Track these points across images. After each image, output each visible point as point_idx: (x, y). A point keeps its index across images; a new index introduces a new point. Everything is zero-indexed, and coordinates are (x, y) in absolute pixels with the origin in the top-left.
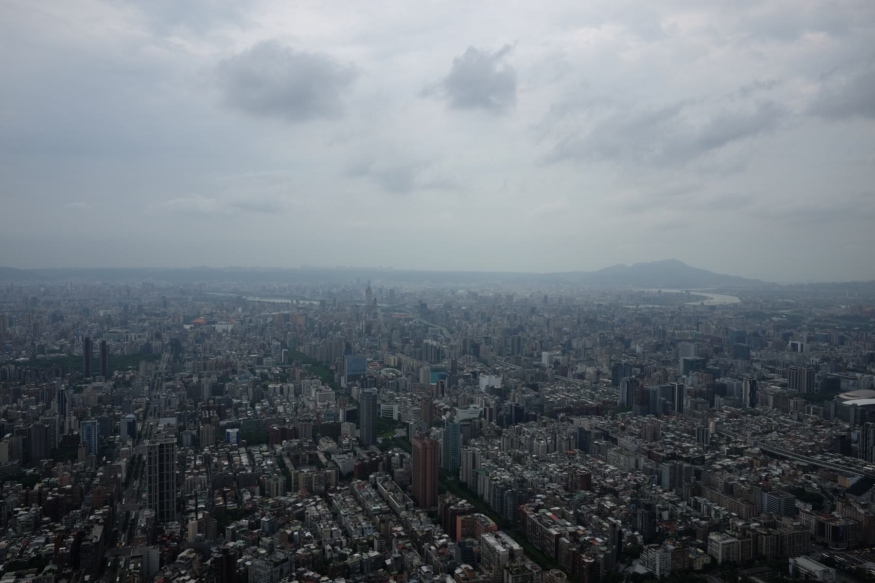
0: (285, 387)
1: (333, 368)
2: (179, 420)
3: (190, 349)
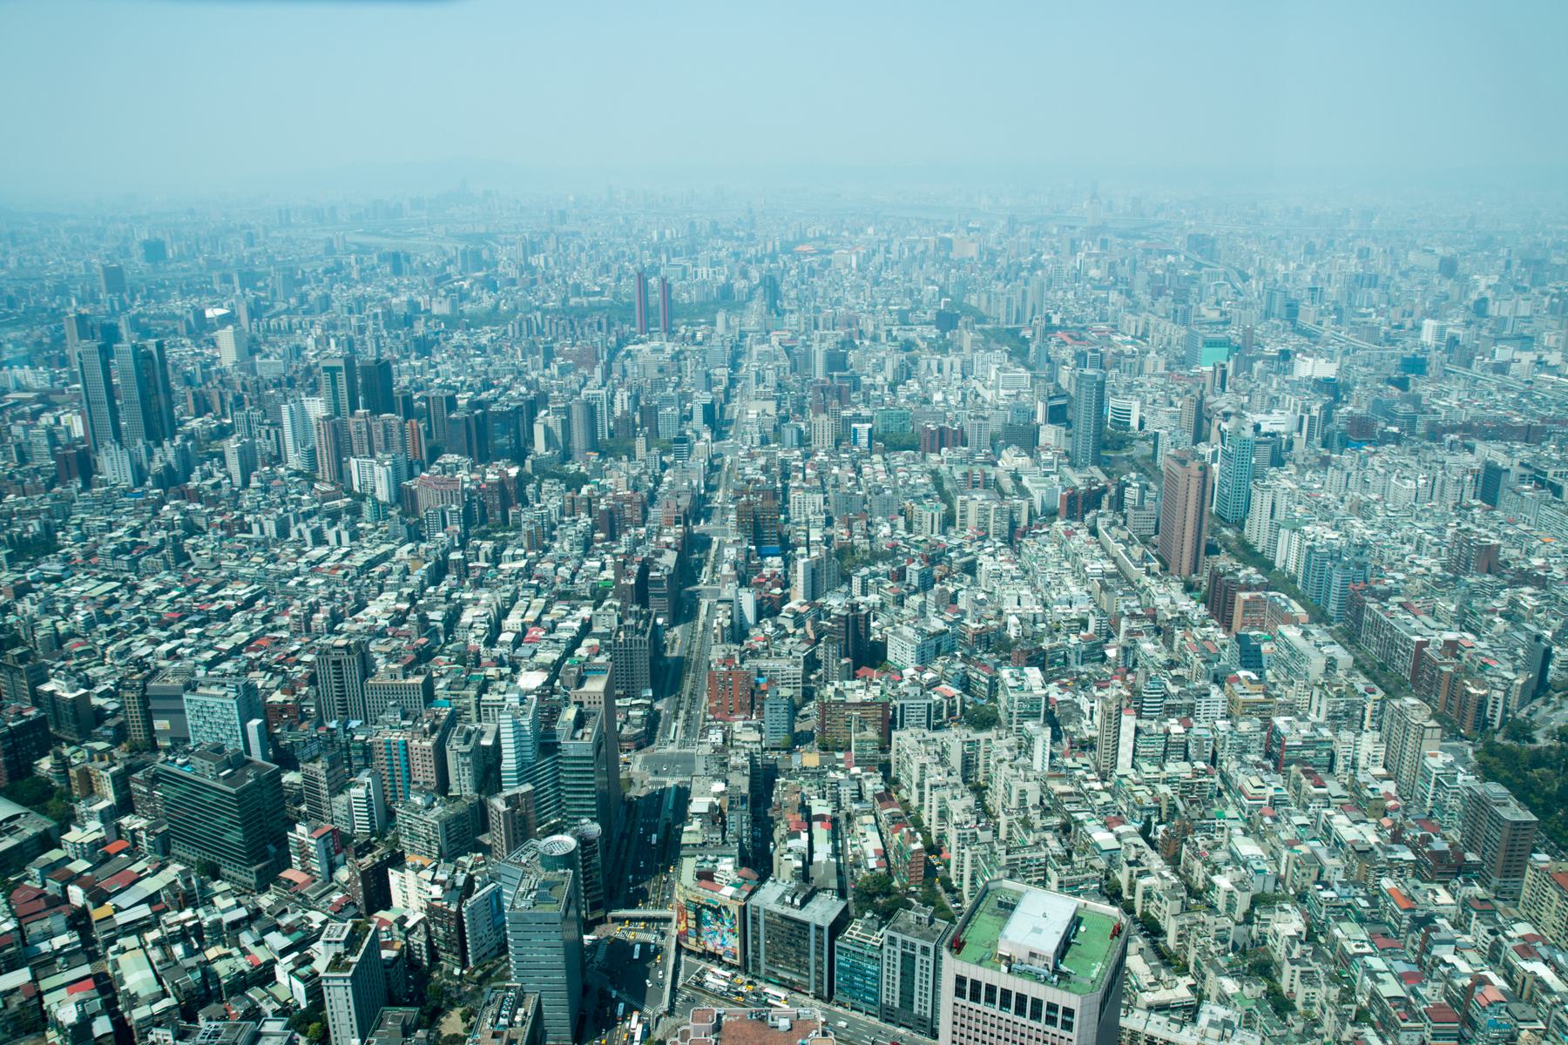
0: (947, 361)
1: (1028, 334)
2: (779, 407)
3: (792, 294)
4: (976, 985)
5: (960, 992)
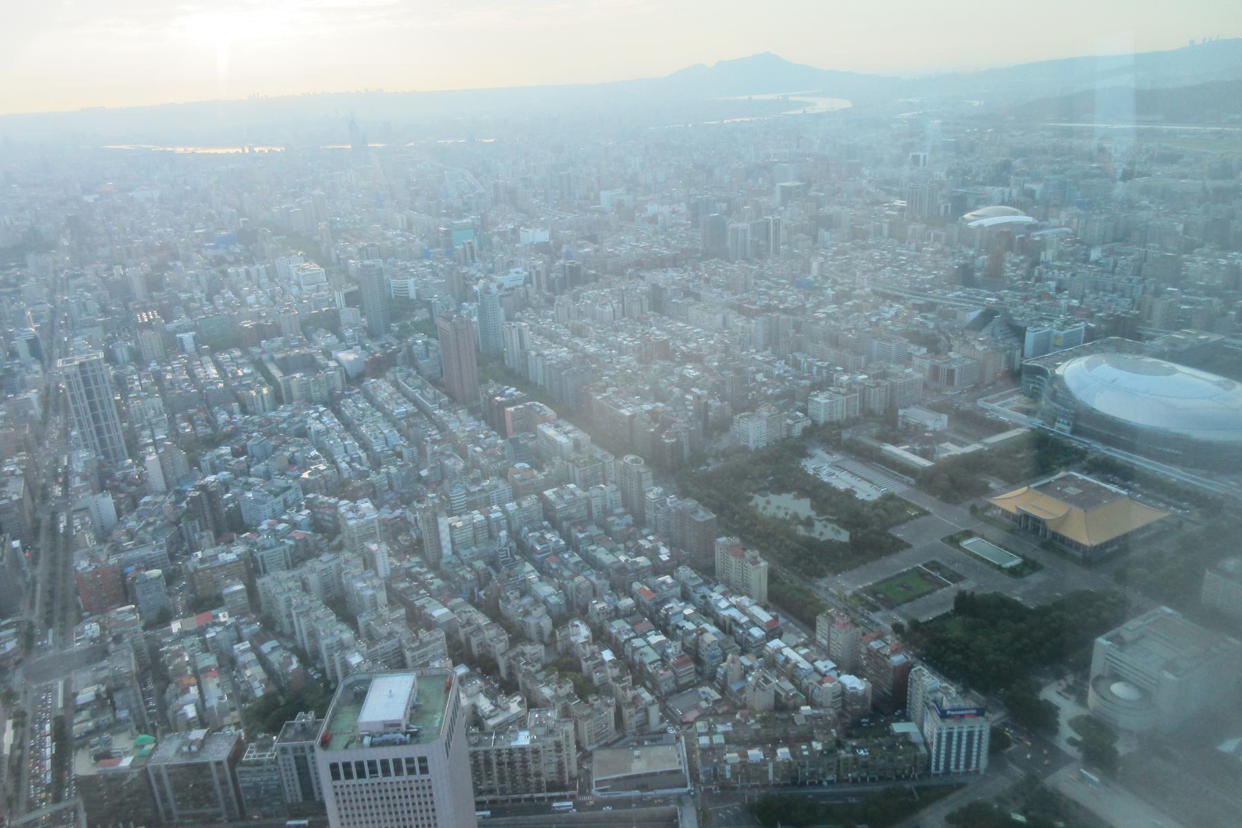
0: (253, 270)
2: (106, 330)
4: (347, 765)
5: (335, 776)
